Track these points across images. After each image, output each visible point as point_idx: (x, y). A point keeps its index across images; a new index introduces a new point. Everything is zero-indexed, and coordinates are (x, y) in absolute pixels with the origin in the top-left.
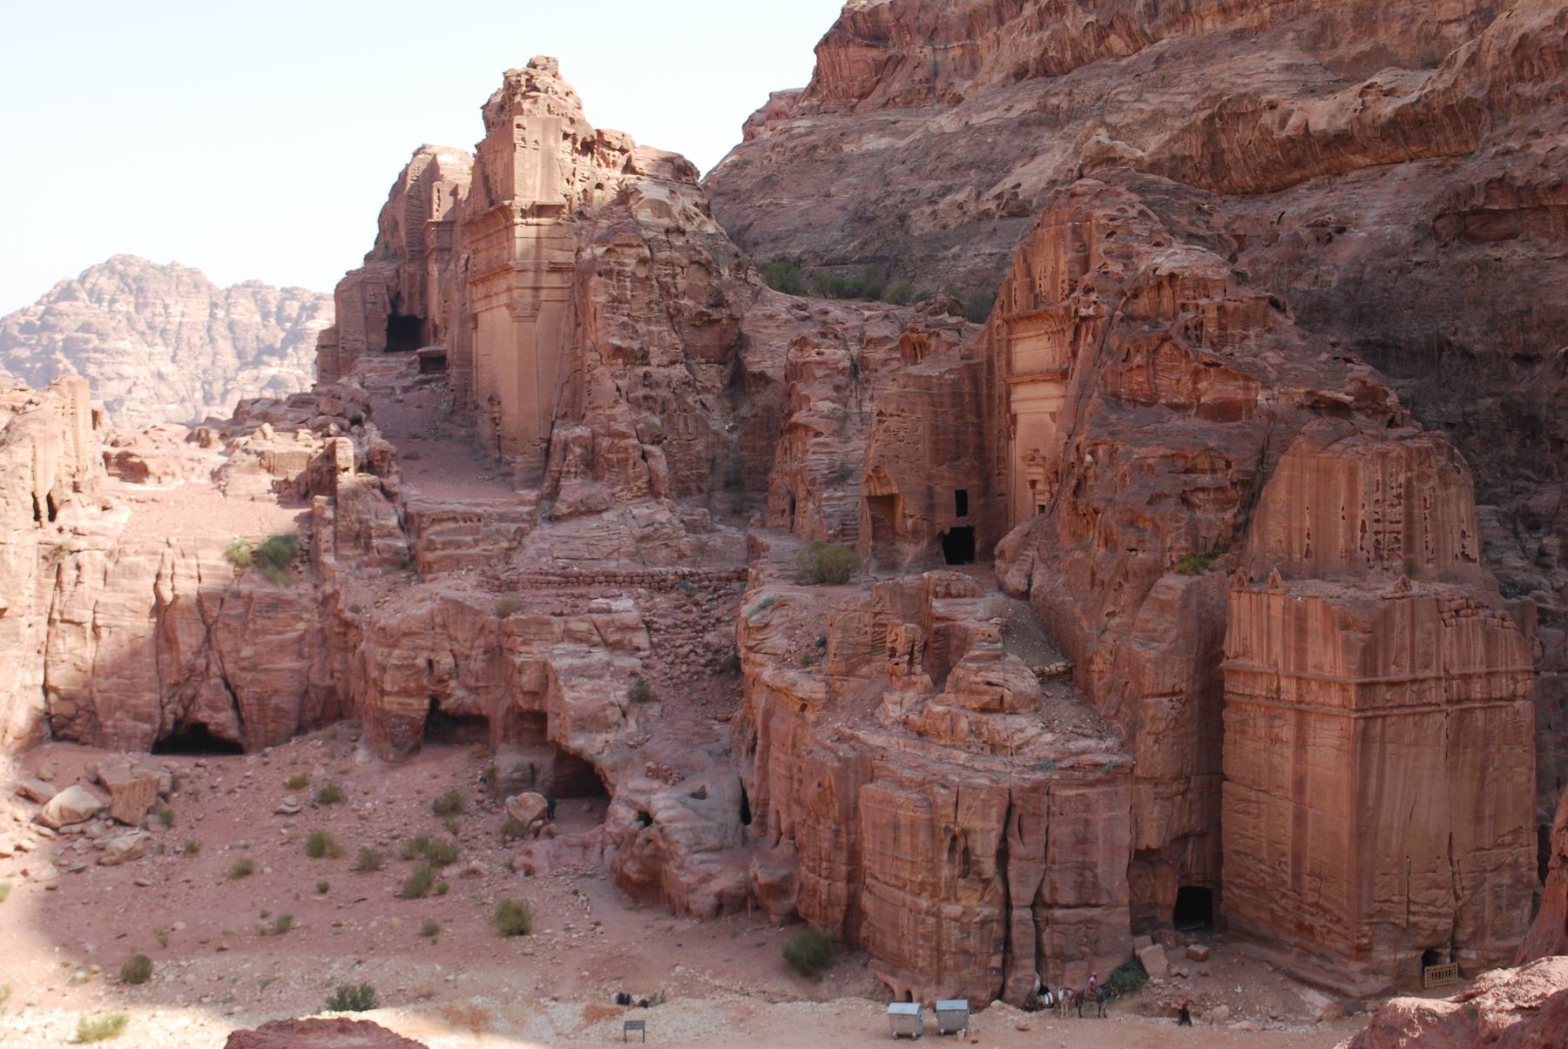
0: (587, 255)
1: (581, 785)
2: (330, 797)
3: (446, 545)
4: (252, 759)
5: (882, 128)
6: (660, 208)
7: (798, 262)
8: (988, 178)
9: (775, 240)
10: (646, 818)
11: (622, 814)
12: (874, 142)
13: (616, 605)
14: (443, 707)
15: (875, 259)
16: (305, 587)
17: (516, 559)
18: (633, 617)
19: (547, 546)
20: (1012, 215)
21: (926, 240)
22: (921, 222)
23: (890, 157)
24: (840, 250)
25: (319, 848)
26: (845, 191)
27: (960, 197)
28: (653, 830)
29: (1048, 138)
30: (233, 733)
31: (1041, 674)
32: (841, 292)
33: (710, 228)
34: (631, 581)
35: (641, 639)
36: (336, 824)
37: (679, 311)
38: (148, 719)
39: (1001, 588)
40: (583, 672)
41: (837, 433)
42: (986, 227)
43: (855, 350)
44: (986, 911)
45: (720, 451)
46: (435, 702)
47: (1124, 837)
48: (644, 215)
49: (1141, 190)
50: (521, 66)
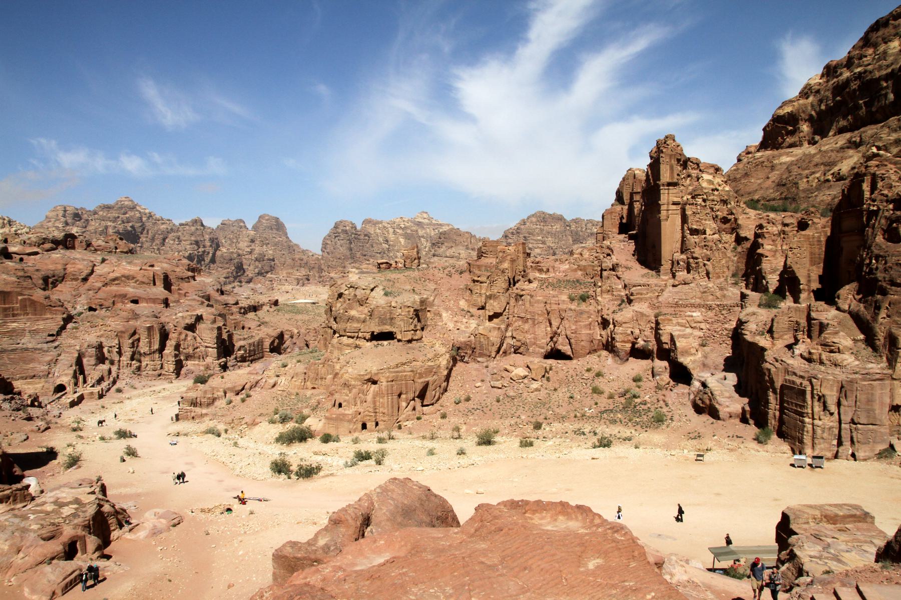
0: (685, 198)
1: (681, 375)
2: (599, 375)
3: (637, 294)
4: (574, 361)
5: (787, 154)
6: (710, 182)
7: (758, 201)
8: (828, 168)
9: (749, 193)
10: (704, 385)
11: (696, 384)
12: (785, 159)
13: (694, 314)
14: (636, 346)
15: (786, 198)
16: (592, 308)
17: (660, 299)
18: (700, 319)
19: (669, 295)
20: (838, 180)
21: (804, 191)
22: (803, 185)
23: (792, 163)
24: (772, 196)
25: (596, 390)
26: (774, 176)
27: (817, 175)
28: (707, 390)
29: (851, 152)
30: (569, 353)
31: (854, 340)
32: (774, 209)
33: (727, 188)
34: (699, 306)
35: (703, 326)
36: (601, 383)
37: (717, 216)
38: (543, 348)
39: (838, 309)
40: (684, 336)
41: (773, 256)
42: (827, 184)
43: (780, 227)
44: (831, 424)
45: (730, 263)
46: (634, 344)
47: (887, 400)
48: (704, 185)
49: (895, 163)
50: (662, 138)
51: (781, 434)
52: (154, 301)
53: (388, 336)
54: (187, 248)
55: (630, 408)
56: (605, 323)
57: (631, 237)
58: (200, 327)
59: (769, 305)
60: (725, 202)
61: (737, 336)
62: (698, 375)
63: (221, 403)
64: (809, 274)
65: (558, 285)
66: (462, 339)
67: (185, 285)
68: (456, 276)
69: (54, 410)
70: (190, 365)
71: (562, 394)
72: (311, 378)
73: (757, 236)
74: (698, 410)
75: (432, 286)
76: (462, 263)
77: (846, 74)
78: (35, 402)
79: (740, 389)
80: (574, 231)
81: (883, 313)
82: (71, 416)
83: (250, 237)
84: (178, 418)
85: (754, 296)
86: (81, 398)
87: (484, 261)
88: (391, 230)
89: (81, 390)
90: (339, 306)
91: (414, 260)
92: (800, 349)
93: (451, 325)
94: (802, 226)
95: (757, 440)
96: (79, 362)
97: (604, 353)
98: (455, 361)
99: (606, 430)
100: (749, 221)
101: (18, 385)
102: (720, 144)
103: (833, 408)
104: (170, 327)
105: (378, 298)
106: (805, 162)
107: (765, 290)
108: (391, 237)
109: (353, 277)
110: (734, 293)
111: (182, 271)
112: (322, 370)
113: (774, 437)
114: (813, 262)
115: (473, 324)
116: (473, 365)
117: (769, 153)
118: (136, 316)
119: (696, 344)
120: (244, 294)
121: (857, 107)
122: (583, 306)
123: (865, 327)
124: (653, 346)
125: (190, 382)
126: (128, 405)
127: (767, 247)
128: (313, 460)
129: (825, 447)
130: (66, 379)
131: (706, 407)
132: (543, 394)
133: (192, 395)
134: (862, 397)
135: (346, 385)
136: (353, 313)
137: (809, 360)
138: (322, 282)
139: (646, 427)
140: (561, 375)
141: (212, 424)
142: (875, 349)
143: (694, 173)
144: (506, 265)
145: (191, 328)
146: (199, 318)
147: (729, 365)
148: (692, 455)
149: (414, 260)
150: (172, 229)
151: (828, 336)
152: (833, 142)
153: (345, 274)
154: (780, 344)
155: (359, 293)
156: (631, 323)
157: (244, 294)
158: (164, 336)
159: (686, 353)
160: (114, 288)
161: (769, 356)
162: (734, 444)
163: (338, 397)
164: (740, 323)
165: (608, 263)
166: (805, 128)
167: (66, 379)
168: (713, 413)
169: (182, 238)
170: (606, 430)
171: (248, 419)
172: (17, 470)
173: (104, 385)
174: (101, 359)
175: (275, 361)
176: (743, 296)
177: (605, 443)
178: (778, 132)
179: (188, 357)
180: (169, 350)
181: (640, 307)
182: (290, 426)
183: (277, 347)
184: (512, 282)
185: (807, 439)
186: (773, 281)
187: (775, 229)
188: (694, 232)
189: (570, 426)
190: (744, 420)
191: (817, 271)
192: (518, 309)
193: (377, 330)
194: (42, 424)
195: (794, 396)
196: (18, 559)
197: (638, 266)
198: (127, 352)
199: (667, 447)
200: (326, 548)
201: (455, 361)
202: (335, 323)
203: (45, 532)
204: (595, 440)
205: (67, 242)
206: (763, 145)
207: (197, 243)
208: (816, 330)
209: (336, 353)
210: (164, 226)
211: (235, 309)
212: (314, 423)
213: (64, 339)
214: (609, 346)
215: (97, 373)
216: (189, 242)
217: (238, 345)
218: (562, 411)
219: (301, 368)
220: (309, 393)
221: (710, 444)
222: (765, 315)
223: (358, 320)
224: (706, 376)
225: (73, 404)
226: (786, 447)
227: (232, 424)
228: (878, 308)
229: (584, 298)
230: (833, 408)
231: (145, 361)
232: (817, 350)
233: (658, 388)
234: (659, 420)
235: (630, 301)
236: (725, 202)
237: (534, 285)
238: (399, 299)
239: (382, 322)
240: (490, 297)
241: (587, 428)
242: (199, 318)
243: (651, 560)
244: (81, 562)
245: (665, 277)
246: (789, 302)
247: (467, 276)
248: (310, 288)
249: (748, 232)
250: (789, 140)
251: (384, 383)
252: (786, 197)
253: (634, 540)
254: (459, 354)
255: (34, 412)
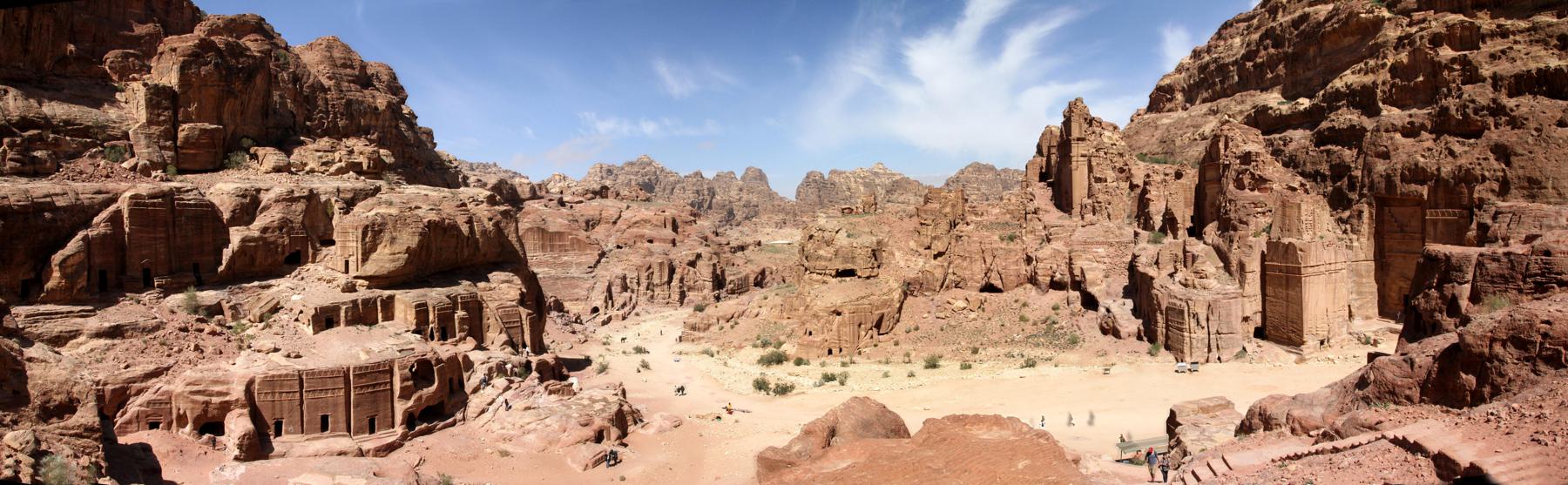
1: (1090, 302)
2: (1025, 305)
10: (1108, 310)
11: (1102, 310)
12: (1165, 121)
19: (1080, 234)
22: (1178, 142)
25: (1022, 319)
26: (1158, 134)
32: (1158, 162)
34: (1102, 243)
36: (1026, 312)
40: (1092, 269)
51: (1167, 348)
52: (664, 241)
53: (850, 273)
54: (691, 197)
55: (1053, 335)
56: (1029, 260)
57: (1049, 185)
58: (700, 263)
59: (1156, 241)
60: (1121, 155)
61: (1132, 267)
62: (1104, 302)
63: (714, 329)
64: (1184, 215)
65: (990, 227)
66: (912, 275)
67: (688, 228)
68: (907, 220)
69: (590, 326)
70: (691, 295)
71: (995, 322)
72: (787, 309)
73: (1146, 183)
74: (1105, 332)
75: (887, 229)
76: (912, 208)
77: (1207, 58)
78: (578, 320)
79: (1136, 312)
80: (1003, 179)
81: (1235, 245)
82: (602, 332)
84: (681, 339)
85: (1144, 234)
86: (610, 319)
87: (929, 206)
89: (610, 312)
90: (810, 246)
91: (872, 206)
92: (1179, 276)
93: (902, 264)
94: (1179, 175)
95: (1150, 353)
96: (609, 290)
97: (1029, 286)
98: (906, 295)
99: (1031, 353)
100: (1139, 171)
101: (567, 305)
102: (1118, 108)
103: (1204, 323)
104: (676, 263)
105: (842, 240)
106: (1179, 124)
107: (1153, 229)
109: (822, 221)
110: (1129, 231)
111: (685, 216)
112: (796, 303)
113: (1163, 349)
114: (1186, 206)
115: (921, 262)
116: (921, 299)
117: (1153, 115)
118: (651, 253)
119: (1101, 276)
120: (734, 236)
121: (1214, 84)
122: (1012, 246)
123: (1223, 256)
124: (1067, 279)
125: (690, 310)
126: (644, 327)
127: (1153, 193)
128: (789, 380)
129: (1199, 355)
130: (599, 303)
131: (1110, 330)
132: (979, 323)
133: (692, 321)
134: (1223, 313)
135: (815, 316)
136: (821, 252)
137: (1186, 286)
138: (796, 226)
139: (1063, 348)
140: (994, 306)
141: (707, 346)
142: (1231, 274)
143: (1098, 130)
144: (948, 210)
145: (692, 264)
146: (699, 256)
147: (1128, 293)
148: (1101, 370)
149: (872, 206)
151: (1199, 266)
152: (1199, 109)
153: (815, 218)
154: (1165, 273)
155: (826, 234)
156: (1050, 260)
157: (734, 236)
158: (672, 271)
159: (1094, 283)
160: (635, 230)
161: (1156, 283)
162: (1132, 358)
163: (809, 327)
164: (1135, 257)
165: (1031, 207)
166: (1179, 96)
167: (599, 303)
168: (1116, 333)
170: (1031, 353)
171: (736, 343)
172: (565, 371)
173: (627, 309)
174: (625, 288)
175: (757, 294)
176: (1136, 234)
177: (1030, 364)
178: (1160, 98)
179: (690, 289)
180: (675, 282)
181: (1057, 245)
182: (770, 350)
183: (760, 282)
184: (953, 225)
185: (1186, 350)
186: (1158, 221)
187: (1158, 178)
188: (1098, 180)
189: (1002, 350)
190: (1140, 338)
191: (1190, 212)
192: (958, 249)
193: (841, 268)
194: (582, 337)
195: (1175, 315)
196: (564, 437)
197: (1054, 209)
198: (644, 283)
199: (1080, 364)
200: (799, 454)
201: (906, 295)
202: (806, 262)
203: (583, 420)
204: (1022, 361)
205: (602, 192)
206: (1150, 109)
208: (1190, 260)
209: (807, 288)
211: (727, 248)
212: (789, 348)
213: (597, 271)
214: (1033, 280)
215: (621, 298)
217: (728, 279)
218: (995, 338)
219: (778, 300)
220: (785, 322)
221: (1114, 360)
222: (1152, 249)
223: (825, 259)
224: (1109, 302)
225: (604, 323)
226: (1171, 357)
227: (723, 347)
228: (1232, 241)
229: (1012, 238)
230: (1204, 323)
231: (657, 291)
232: (1191, 277)
233: (1073, 314)
234: (1074, 342)
235: (1049, 240)
236: (1121, 155)
237: (971, 227)
238: (860, 240)
239: (845, 260)
240: (934, 238)
241: (1016, 352)
242: (699, 256)
243: (1069, 458)
244: (607, 446)
245: (1076, 219)
246: (1169, 239)
247: (915, 219)
248: (787, 230)
249: (1139, 180)
250: (1168, 106)
251: (846, 315)
252: (1167, 152)
253: (1055, 443)
254: (909, 288)
255: (577, 327)
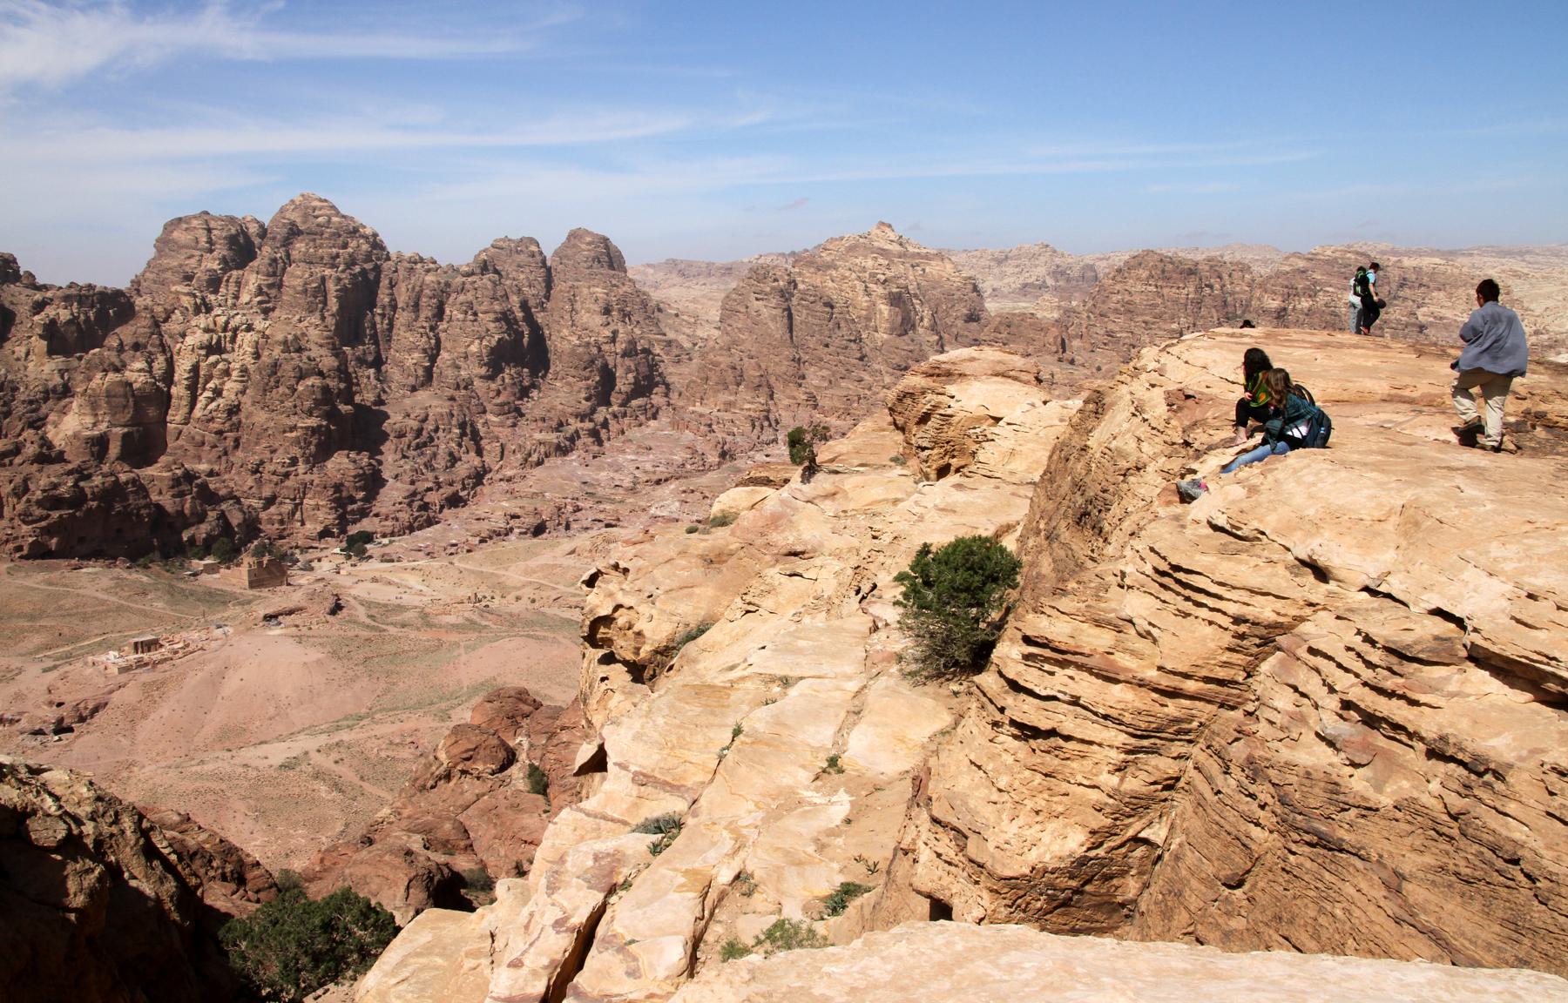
83: (602, 304)
88: (860, 286)
108: (863, 300)
150: (448, 285)
169: (476, 307)
207: (505, 318)
210: (429, 278)
216: (492, 316)
